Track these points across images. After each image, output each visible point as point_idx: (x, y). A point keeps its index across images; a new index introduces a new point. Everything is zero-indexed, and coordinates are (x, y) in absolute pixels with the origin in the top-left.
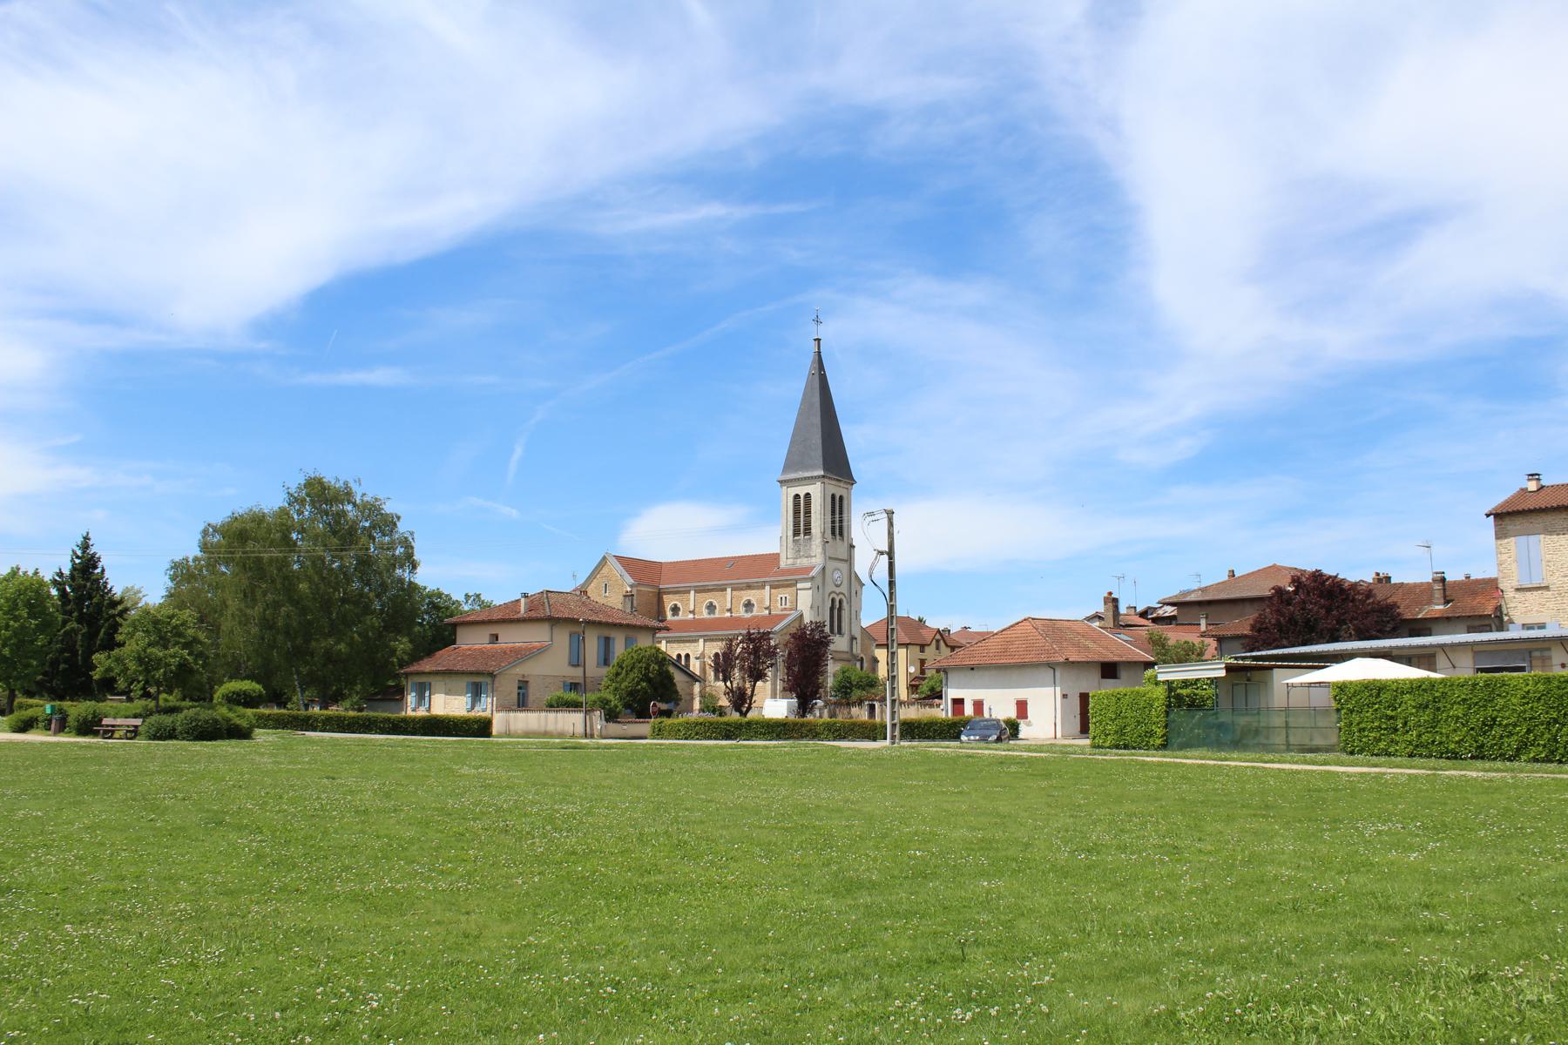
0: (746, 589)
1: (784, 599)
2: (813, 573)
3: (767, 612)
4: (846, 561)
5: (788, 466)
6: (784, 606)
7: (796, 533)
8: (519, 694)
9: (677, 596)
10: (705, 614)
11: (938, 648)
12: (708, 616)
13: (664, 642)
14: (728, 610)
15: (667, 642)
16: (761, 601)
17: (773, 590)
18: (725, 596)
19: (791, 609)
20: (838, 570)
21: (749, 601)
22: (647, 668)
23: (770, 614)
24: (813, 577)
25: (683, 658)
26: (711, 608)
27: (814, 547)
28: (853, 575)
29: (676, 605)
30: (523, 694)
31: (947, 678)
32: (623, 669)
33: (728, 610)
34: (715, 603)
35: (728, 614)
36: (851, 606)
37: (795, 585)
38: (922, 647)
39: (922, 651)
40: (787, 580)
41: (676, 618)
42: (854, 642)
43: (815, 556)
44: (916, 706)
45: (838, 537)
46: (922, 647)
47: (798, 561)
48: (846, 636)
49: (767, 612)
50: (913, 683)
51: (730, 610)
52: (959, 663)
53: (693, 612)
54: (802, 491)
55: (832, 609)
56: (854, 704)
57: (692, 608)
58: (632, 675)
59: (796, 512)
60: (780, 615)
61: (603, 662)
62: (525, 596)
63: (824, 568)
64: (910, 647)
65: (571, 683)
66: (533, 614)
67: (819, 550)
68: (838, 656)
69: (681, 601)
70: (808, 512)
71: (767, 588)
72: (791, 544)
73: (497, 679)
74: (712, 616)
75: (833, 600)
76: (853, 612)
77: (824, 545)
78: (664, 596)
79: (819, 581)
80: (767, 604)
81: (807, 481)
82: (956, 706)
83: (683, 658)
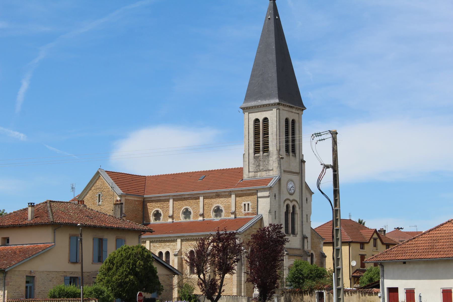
1: (247, 205)
2: (270, 184)
3: (233, 216)
5: (248, 97)
6: (247, 211)
7: (256, 151)
8: (27, 287)
9: (158, 204)
10: (182, 219)
11: (375, 245)
12: (185, 220)
13: (148, 242)
15: (150, 242)
16: (229, 207)
17: (238, 198)
18: (198, 204)
19: (253, 214)
20: (292, 181)
21: (218, 208)
22: (134, 264)
23: (235, 217)
24: (270, 188)
25: (164, 255)
26: (187, 213)
27: (271, 162)
28: (304, 185)
29: (157, 211)
30: (31, 287)
31: (383, 271)
32: (113, 265)
34: (190, 209)
35: (201, 219)
36: (302, 211)
37: (256, 194)
38: (362, 245)
40: (249, 190)
41: (158, 222)
42: (306, 240)
43: (272, 170)
44: (358, 294)
45: (291, 154)
46: (362, 245)
47: (259, 174)
49: (233, 216)
50: (355, 274)
51: (202, 215)
52: (393, 258)
53: (172, 217)
54: (261, 116)
55: (287, 213)
56: (305, 292)
57: (171, 213)
58: (121, 270)
59: (256, 134)
61: (97, 259)
62: (32, 205)
63: (280, 180)
64: (352, 245)
65: (71, 278)
66: (39, 220)
68: (291, 252)
70: (266, 133)
71: (233, 196)
72: (252, 160)
73: (8, 275)
74: (188, 220)
75: (288, 206)
76: (305, 216)
78: (148, 204)
79: (276, 190)
80: (233, 209)
82: (391, 294)
83: (164, 255)
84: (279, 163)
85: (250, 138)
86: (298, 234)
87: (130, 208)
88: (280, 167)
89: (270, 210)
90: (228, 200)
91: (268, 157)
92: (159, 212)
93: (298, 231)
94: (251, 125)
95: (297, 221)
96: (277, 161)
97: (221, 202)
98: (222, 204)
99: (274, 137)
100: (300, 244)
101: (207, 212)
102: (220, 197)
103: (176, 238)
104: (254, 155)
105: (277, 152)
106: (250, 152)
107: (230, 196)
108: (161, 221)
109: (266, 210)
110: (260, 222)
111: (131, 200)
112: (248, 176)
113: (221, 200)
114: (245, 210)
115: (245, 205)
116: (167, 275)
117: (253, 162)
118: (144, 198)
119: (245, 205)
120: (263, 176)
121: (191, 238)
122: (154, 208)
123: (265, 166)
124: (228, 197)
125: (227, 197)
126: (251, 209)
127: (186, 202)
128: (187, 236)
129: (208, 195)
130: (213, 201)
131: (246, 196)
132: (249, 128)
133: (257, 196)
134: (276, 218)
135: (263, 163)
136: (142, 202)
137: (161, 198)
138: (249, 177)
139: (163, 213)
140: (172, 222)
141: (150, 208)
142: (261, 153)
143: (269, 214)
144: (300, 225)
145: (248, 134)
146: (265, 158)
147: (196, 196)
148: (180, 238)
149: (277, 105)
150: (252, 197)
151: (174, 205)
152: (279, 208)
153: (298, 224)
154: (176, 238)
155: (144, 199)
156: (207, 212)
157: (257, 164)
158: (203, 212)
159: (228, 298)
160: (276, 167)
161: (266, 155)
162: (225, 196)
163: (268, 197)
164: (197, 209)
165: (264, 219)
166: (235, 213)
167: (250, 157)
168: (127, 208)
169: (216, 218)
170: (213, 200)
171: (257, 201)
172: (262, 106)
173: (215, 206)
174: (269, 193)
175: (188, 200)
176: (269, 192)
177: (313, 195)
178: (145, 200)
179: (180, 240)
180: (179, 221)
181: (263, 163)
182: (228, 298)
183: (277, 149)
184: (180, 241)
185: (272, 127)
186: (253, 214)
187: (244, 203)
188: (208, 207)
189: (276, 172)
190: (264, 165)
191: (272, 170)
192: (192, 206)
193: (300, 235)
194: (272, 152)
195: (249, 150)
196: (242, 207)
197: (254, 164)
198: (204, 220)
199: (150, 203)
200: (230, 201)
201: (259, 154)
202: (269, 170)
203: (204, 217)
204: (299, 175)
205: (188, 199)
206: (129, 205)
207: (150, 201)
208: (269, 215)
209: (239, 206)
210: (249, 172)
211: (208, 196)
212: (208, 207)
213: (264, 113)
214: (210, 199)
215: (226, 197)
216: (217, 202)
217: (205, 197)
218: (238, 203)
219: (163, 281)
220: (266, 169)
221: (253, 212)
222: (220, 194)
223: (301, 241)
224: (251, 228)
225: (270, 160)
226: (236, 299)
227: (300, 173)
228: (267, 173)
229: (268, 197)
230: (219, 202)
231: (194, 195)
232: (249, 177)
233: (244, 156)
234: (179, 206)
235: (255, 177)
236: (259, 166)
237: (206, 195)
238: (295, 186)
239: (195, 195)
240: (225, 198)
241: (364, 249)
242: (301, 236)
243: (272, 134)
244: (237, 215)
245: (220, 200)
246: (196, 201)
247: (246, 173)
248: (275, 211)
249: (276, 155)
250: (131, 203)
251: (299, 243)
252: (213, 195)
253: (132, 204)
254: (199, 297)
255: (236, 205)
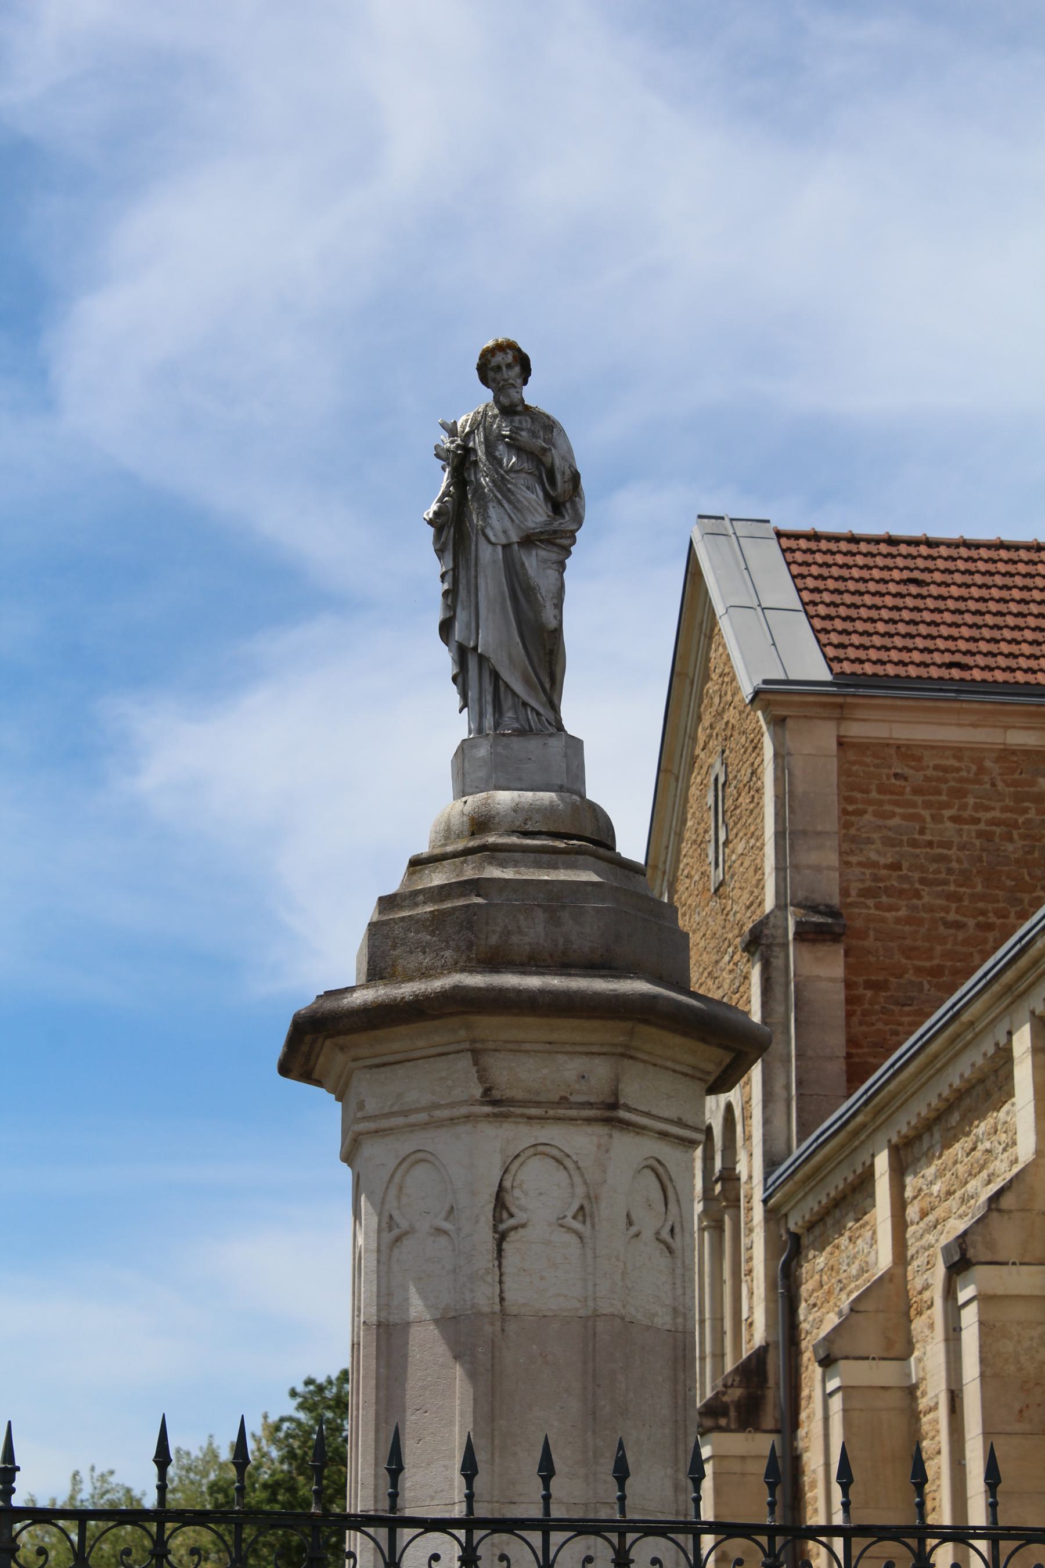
87: (948, 845)
111: (958, 751)
168: (888, 842)
206: (926, 814)
250: (959, 793)
253: (971, 801)
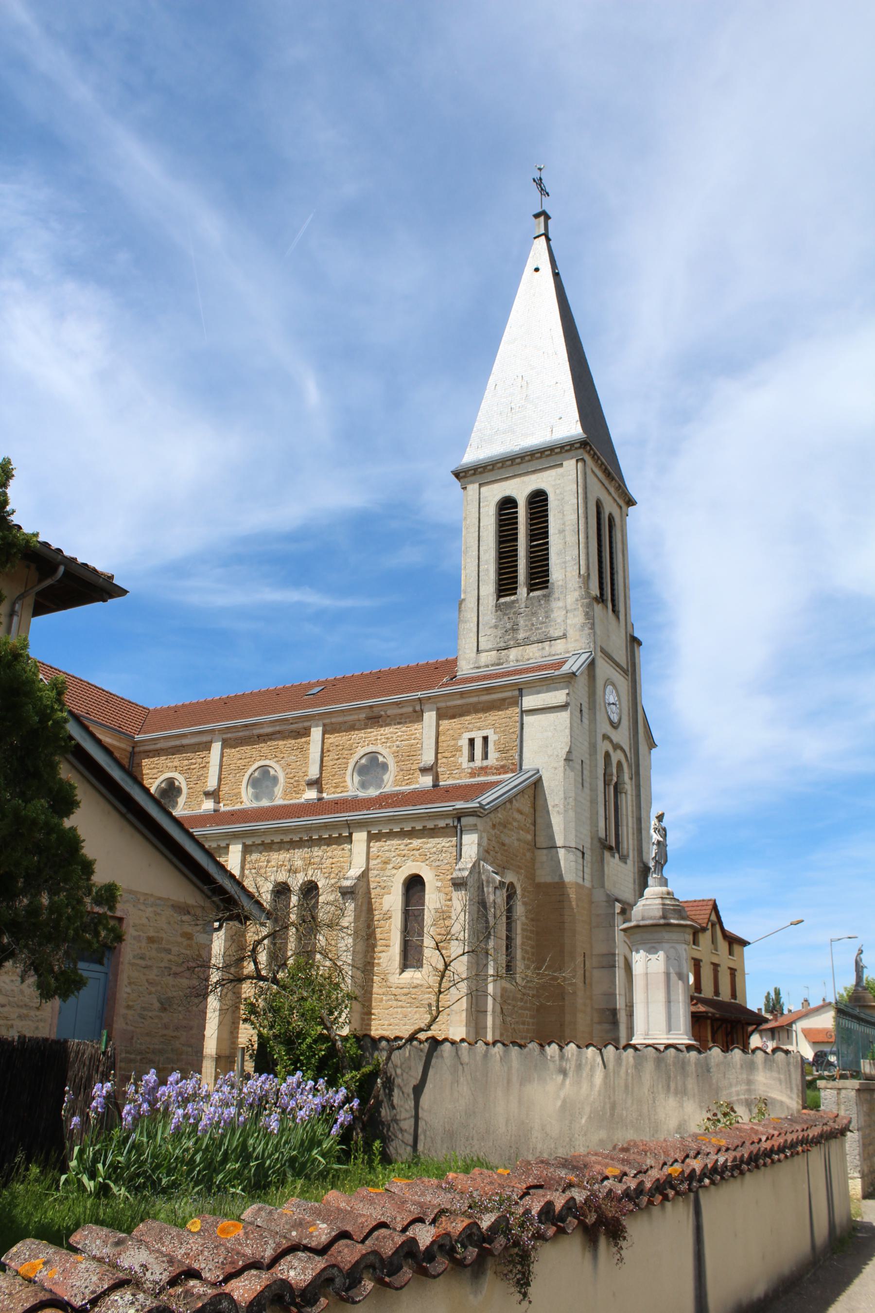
0: (366, 727)
1: (478, 744)
4: (625, 672)
6: (478, 762)
9: (176, 760)
12: (255, 804)
14: (311, 784)
16: (407, 756)
17: (445, 724)
18: (303, 750)
19: (502, 769)
21: (373, 757)
23: (436, 785)
27: (558, 615)
33: (311, 784)
37: (515, 702)
38: (696, 932)
39: (695, 942)
43: (564, 636)
47: (513, 654)
48: (630, 862)
49: (426, 781)
51: (316, 783)
53: (213, 795)
57: (212, 784)
60: (467, 786)
67: (577, 619)
69: (186, 771)
71: (430, 717)
77: (589, 606)
78: (145, 762)
80: (428, 758)
81: (536, 465)
84: (587, 614)
85: (485, 553)
86: (628, 856)
88: (593, 624)
89: (569, 752)
90: (411, 730)
91: (548, 600)
92: (177, 783)
93: (628, 849)
94: (488, 515)
95: (627, 815)
96: (579, 606)
97: (383, 740)
98: (388, 745)
99: (568, 539)
100: (635, 891)
101: (334, 775)
102: (381, 723)
103: (227, 842)
104: (497, 600)
105: (579, 582)
106: (481, 593)
107: (418, 716)
108: (179, 810)
109: (556, 753)
110: (531, 792)
112: (476, 662)
113: (384, 733)
114: (472, 758)
115: (472, 742)
116: (182, 909)
117: (494, 621)
118: (135, 744)
119: (472, 742)
120: (528, 660)
121: (282, 837)
122: (161, 771)
123: (537, 629)
124: (411, 722)
125: (407, 720)
126: (497, 755)
127: (264, 748)
128: (266, 832)
129: (340, 719)
130: (355, 739)
131: (477, 711)
132: (481, 525)
133: (518, 710)
134: (585, 784)
135: (530, 620)
136: (129, 755)
137: (185, 741)
138: (476, 665)
139: (187, 785)
140: (215, 811)
141: (148, 774)
142: (522, 591)
143: (567, 767)
144: (633, 828)
145: (477, 542)
146: (536, 604)
147: (300, 725)
148: (241, 841)
149: (580, 448)
150: (500, 713)
151: (224, 759)
152: (590, 755)
153: (627, 826)
154: (227, 842)
155: (133, 748)
156: (334, 775)
157: (509, 626)
158: (321, 773)
159: (619, 1060)
160: (578, 626)
161: (538, 596)
162: (401, 720)
163: (564, 707)
164: (299, 767)
165: (546, 784)
166: (434, 770)
167: (481, 608)
169: (363, 791)
170: (356, 735)
171: (518, 724)
172: (527, 458)
173: (362, 753)
174: (568, 694)
175: (271, 739)
176: (567, 691)
177: (653, 751)
178: (137, 749)
179: (239, 847)
180: (238, 807)
181: (530, 620)
182: (619, 1060)
183: (580, 573)
184: (241, 849)
185: (562, 512)
186: (502, 769)
187: (467, 736)
188: (336, 757)
189: (576, 640)
190: (533, 625)
191: (564, 636)
192: (283, 758)
193: (634, 862)
194: (560, 583)
195: (480, 587)
196: (459, 749)
197: (496, 627)
198: (320, 799)
199: (151, 760)
200: (418, 735)
201: (513, 598)
202: (552, 640)
203: (320, 791)
204: (626, 677)
205: (270, 737)
207: (150, 751)
208: (565, 770)
209: (448, 746)
210: (478, 650)
211: (340, 723)
212: (339, 759)
213: (533, 477)
214: (344, 731)
215: (403, 720)
216: (370, 741)
217: (328, 729)
218: (448, 738)
219: (151, 940)
220: (542, 637)
221: (502, 763)
222: (383, 713)
223: (637, 881)
224: (508, 805)
225: (555, 610)
226: (691, 1069)
227: (630, 673)
228: (543, 648)
229: (564, 707)
230: (377, 739)
231: (292, 724)
232: (478, 668)
233: (463, 605)
234: (240, 761)
235: (498, 664)
236: (514, 629)
237: (334, 720)
238: (620, 704)
239: (296, 723)
240: (399, 726)
241: (698, 946)
242: (636, 863)
243: (562, 531)
244: (441, 777)
245: (382, 732)
246: (296, 741)
247: (467, 656)
248: (582, 761)
249: (575, 590)
251: (631, 886)
252: (356, 717)
254: (391, 1051)
255: (440, 744)
